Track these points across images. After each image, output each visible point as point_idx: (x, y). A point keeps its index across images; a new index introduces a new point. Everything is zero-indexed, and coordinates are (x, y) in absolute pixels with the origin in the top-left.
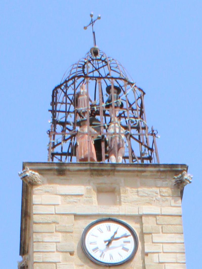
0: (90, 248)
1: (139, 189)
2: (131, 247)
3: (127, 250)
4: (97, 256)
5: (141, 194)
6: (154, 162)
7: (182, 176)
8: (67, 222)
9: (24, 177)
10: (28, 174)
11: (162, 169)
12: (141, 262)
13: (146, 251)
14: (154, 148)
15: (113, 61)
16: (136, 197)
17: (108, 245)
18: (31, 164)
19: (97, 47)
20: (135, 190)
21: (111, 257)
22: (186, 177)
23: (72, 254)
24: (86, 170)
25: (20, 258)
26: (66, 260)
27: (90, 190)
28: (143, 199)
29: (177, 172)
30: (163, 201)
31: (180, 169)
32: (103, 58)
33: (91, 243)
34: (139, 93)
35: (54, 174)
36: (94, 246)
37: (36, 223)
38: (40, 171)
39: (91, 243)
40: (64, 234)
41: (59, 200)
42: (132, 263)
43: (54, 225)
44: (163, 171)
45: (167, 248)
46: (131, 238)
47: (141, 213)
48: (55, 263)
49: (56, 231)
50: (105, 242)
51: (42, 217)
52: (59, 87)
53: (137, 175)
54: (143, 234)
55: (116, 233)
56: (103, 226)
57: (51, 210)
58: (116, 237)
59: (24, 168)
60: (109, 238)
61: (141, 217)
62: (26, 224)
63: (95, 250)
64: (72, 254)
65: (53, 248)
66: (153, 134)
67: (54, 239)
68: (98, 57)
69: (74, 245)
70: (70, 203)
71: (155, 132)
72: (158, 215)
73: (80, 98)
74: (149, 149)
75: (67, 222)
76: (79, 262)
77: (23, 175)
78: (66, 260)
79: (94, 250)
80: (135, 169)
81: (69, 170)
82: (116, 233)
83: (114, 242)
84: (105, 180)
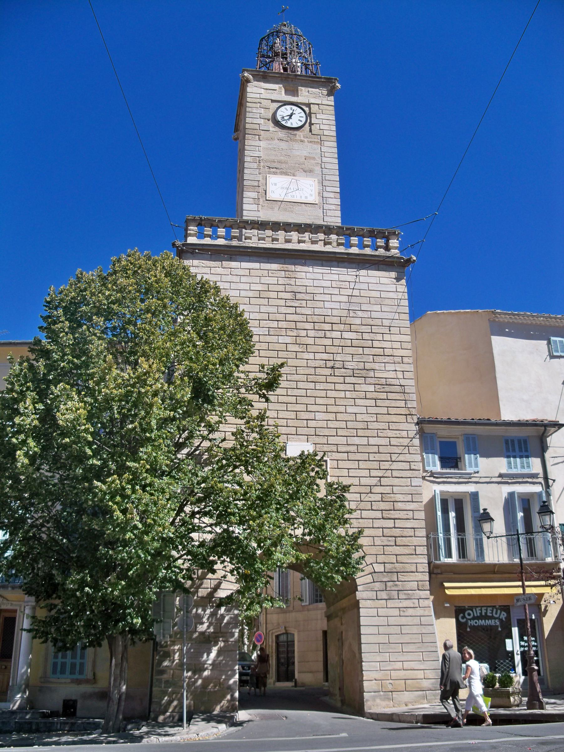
0: (279, 118)
2: (304, 120)
3: (301, 121)
13: (313, 122)
20: (307, 90)
21: (292, 124)
41: (263, 91)
43: (259, 104)
52: (264, 38)
64: (269, 120)
69: (270, 115)
75: (267, 103)
80: (308, 79)
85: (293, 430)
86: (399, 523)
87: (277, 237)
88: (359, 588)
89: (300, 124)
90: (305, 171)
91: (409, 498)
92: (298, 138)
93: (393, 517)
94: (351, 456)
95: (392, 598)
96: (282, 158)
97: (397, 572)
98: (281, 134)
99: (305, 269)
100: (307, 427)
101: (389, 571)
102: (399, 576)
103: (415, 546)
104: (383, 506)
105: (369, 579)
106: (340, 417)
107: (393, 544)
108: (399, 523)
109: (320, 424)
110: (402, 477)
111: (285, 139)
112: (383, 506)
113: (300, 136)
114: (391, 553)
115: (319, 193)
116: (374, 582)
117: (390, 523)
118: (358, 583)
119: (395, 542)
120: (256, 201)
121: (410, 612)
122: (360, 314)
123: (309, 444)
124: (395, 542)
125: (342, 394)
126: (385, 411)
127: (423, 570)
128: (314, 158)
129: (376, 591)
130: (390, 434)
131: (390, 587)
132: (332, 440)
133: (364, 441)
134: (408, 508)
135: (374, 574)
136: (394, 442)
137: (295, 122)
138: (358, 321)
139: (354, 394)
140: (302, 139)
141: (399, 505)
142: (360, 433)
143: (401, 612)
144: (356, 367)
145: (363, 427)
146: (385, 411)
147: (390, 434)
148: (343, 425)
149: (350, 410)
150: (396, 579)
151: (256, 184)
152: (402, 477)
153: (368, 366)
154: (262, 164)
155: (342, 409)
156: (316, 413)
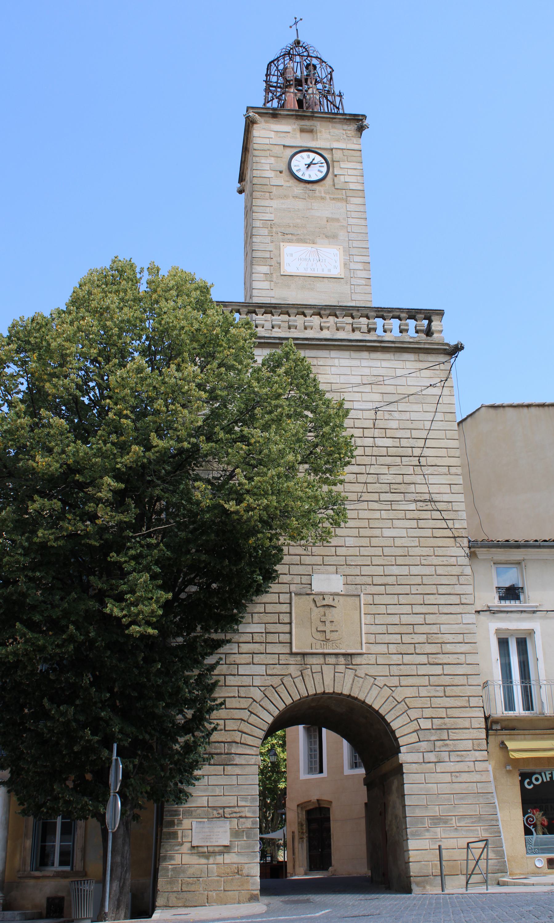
0: (294, 169)
1: (331, 131)
2: (324, 170)
3: (321, 172)
4: (299, 175)
5: (332, 134)
6: (341, 111)
7: (363, 122)
8: (278, 150)
9: (248, 117)
10: (250, 114)
11: (347, 117)
12: (332, 181)
13: (336, 173)
14: (340, 107)
15: (311, 48)
16: (328, 136)
17: (308, 168)
18: (253, 108)
19: (299, 39)
20: (328, 131)
21: (310, 176)
22: (365, 123)
23: (281, 172)
24: (292, 115)
25: (239, 185)
26: (276, 176)
27: (295, 129)
28: (333, 137)
29: (359, 120)
30: (348, 140)
31: (361, 118)
32: (304, 45)
33: (295, 166)
34: (329, 70)
35: (269, 117)
36: (298, 168)
37: (255, 150)
38: (258, 113)
39: (295, 166)
40: (276, 158)
41: (272, 135)
42: (324, 182)
43: (268, 152)
44: (349, 119)
45: (351, 172)
46: (325, 165)
47: (332, 147)
48: (269, 178)
49: (270, 156)
50: (306, 165)
51: (260, 145)
52: (273, 62)
53: (330, 121)
54: (333, 161)
55: (314, 159)
56: (305, 154)
57: (267, 141)
58: (313, 162)
59: (247, 111)
60: (308, 163)
61: (332, 149)
62: (245, 158)
63: (299, 170)
64: (281, 172)
65: (267, 167)
66: (340, 96)
67: (268, 161)
68: (301, 45)
69: (283, 166)
70: (280, 137)
71: (342, 94)
72: (345, 149)
73: (287, 70)
74: (337, 108)
75: (278, 150)
76: (287, 178)
77: (247, 115)
78: (276, 176)
79: (297, 171)
80: (329, 116)
81: (280, 114)
82: (314, 159)
83: (312, 166)
84: (307, 123)
85: (319, 560)
86: (448, 670)
87: (295, 324)
88: (402, 749)
89: (321, 176)
90: (327, 237)
91: (460, 638)
92: (317, 194)
93: (440, 662)
94: (389, 589)
95: (441, 761)
96: (299, 221)
97: (448, 729)
98: (299, 189)
99: (329, 362)
100: (337, 556)
101: (438, 727)
102: (450, 734)
103: (469, 696)
104: (429, 648)
105: (414, 737)
106: (375, 542)
107: (442, 694)
108: (448, 670)
109: (352, 551)
110: (451, 614)
111: (301, 197)
112: (429, 648)
113: (320, 192)
114: (439, 706)
115: (345, 264)
116: (420, 741)
117: (438, 670)
118: (401, 743)
119: (445, 692)
120: (268, 277)
121: (464, 777)
122: (396, 415)
123: (339, 576)
124: (445, 692)
125: (377, 515)
126: (428, 533)
127: (479, 726)
128: (337, 220)
129: (423, 752)
130: (435, 561)
131: (440, 747)
132: (366, 570)
133: (404, 570)
134: (459, 651)
135: (419, 732)
136: (440, 570)
137: (314, 174)
138: (394, 424)
139: (392, 514)
140: (323, 195)
141: (448, 648)
142: (400, 561)
143: (453, 777)
144: (394, 481)
145: (403, 554)
146: (428, 533)
147: (435, 561)
148: (379, 551)
149: (387, 533)
150: (446, 738)
151: (267, 255)
152: (451, 614)
153: (407, 479)
154: (274, 229)
155: (377, 532)
156: (347, 539)
